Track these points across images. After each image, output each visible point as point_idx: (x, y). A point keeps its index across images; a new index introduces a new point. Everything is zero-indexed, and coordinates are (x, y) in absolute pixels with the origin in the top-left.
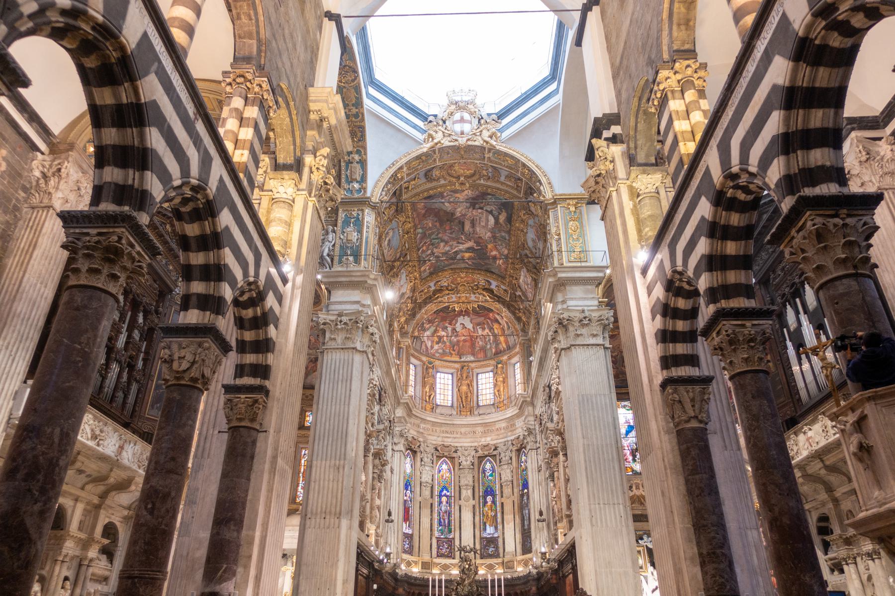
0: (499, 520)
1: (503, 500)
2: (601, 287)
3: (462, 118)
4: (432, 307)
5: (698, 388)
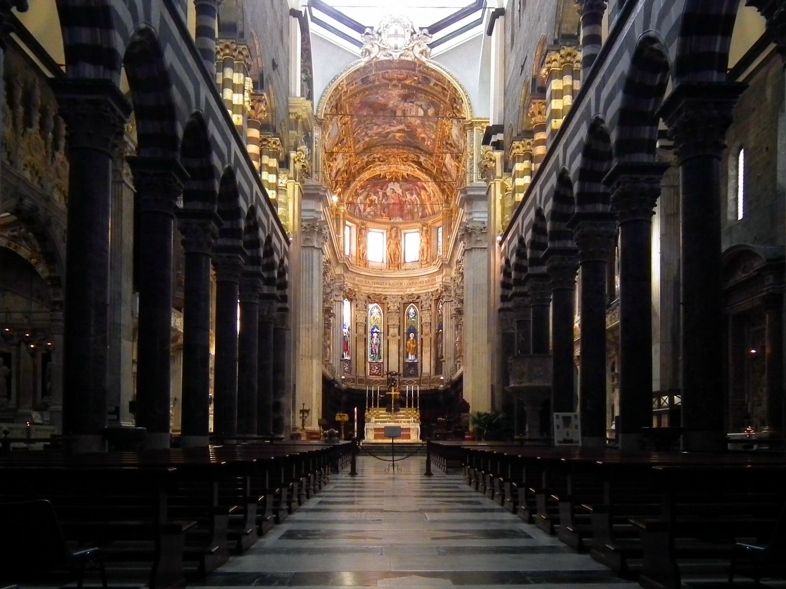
0: (419, 351)
1: (423, 336)
4: (366, 175)
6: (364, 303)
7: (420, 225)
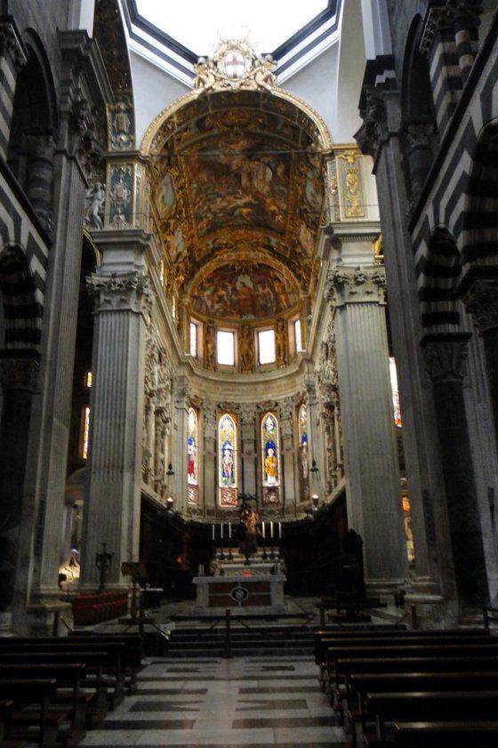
2: (378, 243)
4: (212, 265)
5: (456, 344)
6: (212, 413)
7: (274, 321)
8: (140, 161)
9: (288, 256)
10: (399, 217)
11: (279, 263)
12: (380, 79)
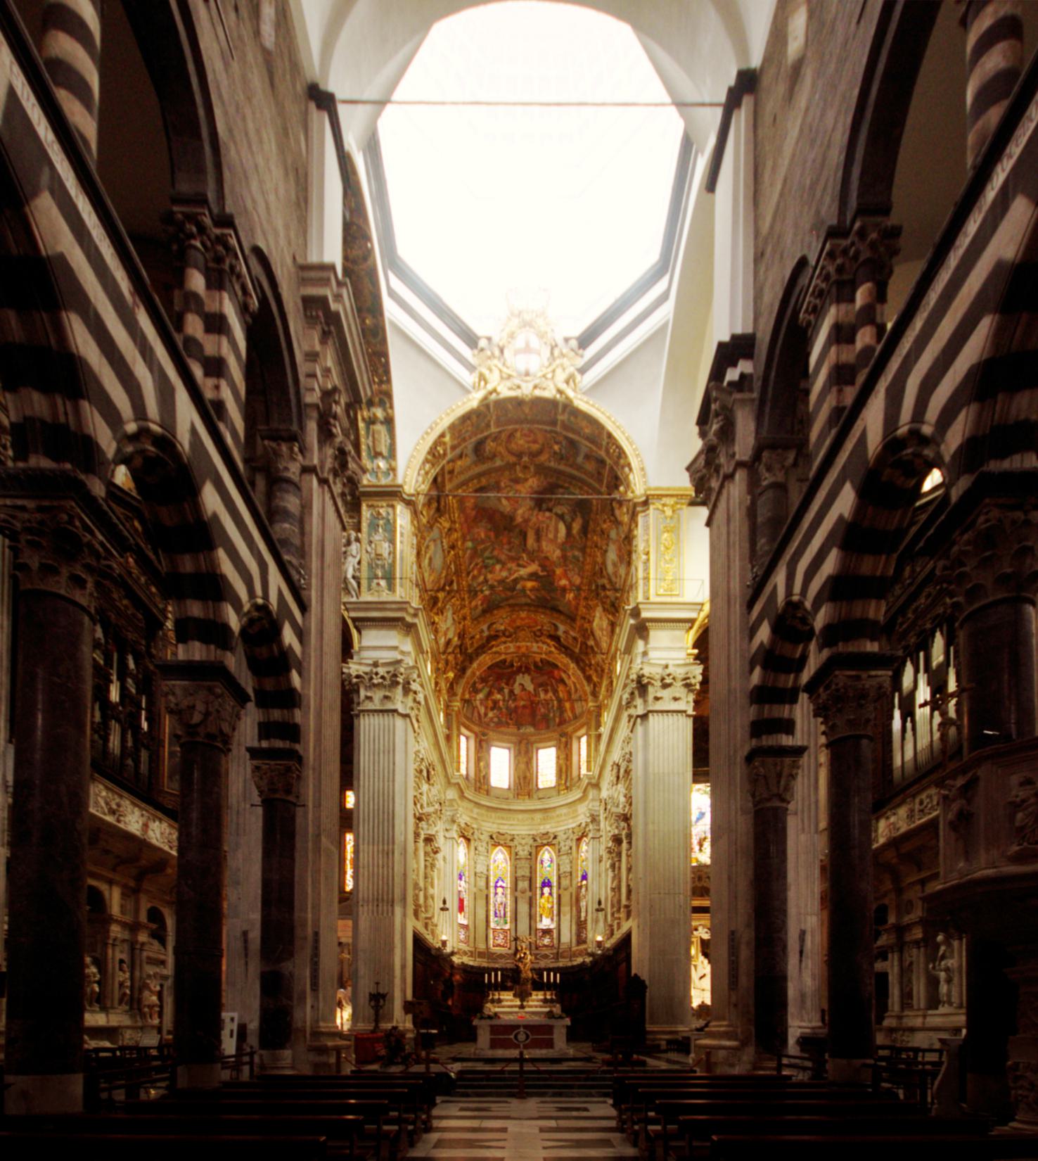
3: (527, 345)
8: (404, 500)
9: (577, 650)
10: (736, 586)
11: (566, 660)
12: (732, 375)
